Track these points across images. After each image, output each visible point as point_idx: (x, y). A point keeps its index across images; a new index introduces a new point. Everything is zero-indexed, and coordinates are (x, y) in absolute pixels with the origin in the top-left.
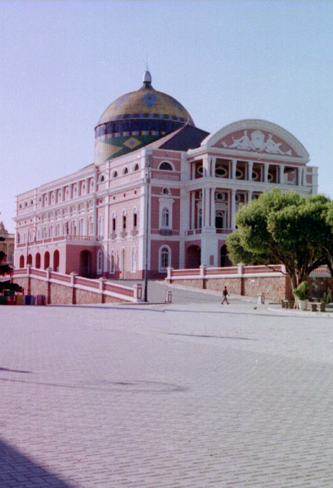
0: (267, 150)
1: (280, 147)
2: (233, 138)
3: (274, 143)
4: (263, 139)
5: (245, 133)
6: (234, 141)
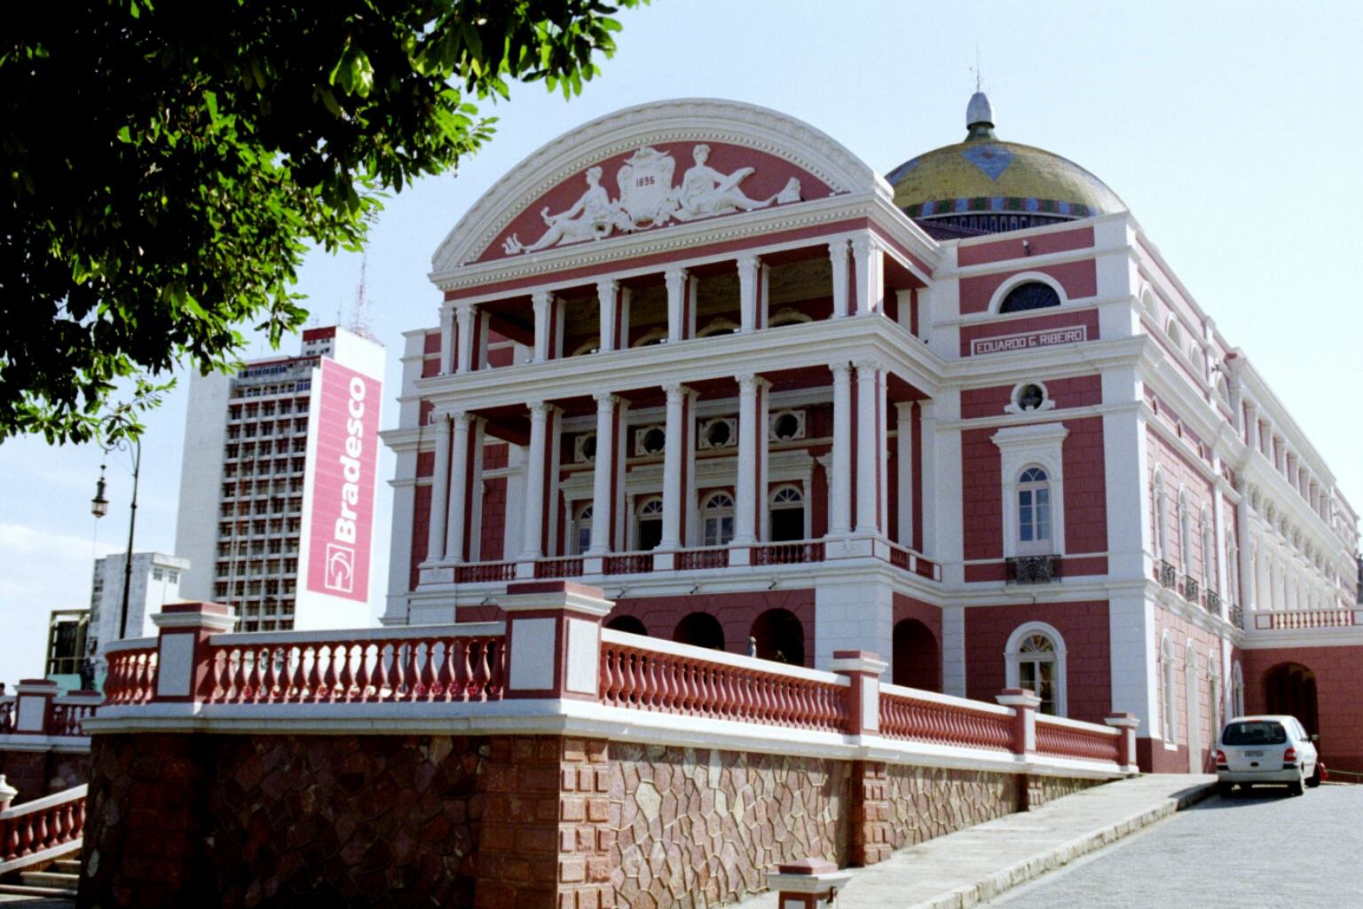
0: (680, 215)
1: (744, 185)
2: (544, 213)
3: (719, 177)
4: (669, 176)
5: (594, 176)
6: (548, 220)
